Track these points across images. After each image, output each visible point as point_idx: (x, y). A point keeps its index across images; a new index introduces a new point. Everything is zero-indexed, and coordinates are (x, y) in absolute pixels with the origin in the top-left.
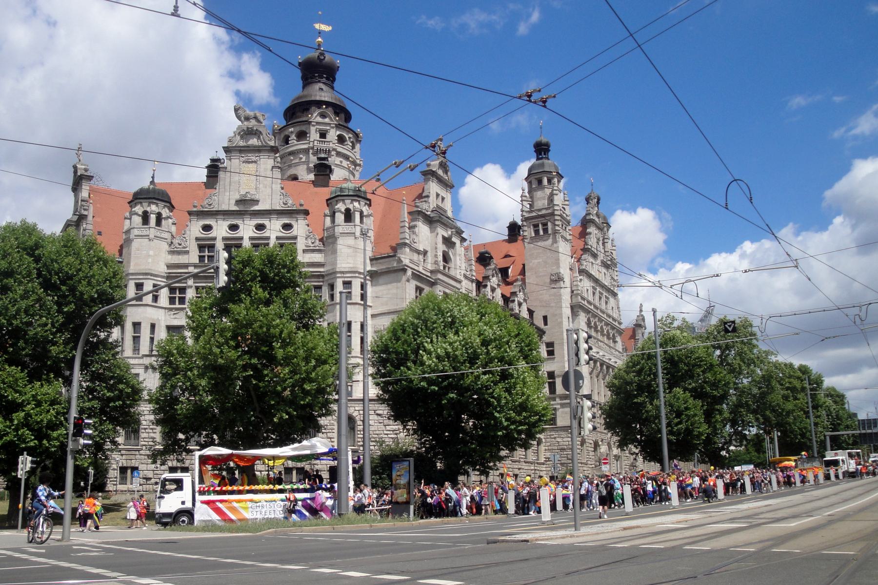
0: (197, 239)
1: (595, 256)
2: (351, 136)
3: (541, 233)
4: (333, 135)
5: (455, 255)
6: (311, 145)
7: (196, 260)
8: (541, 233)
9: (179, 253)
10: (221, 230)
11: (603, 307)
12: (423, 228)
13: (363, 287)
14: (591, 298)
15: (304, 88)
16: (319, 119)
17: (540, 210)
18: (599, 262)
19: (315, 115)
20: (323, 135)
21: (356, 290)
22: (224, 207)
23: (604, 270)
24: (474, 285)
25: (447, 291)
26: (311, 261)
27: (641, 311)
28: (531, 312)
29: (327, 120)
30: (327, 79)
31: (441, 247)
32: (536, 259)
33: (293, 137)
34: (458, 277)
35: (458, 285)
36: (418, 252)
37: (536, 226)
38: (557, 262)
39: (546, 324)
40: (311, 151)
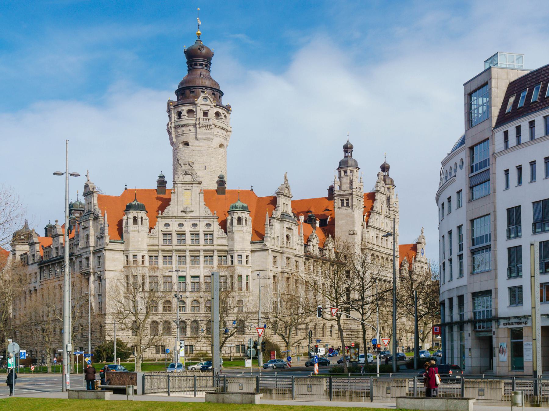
1: (379, 214)
2: (224, 112)
3: (345, 204)
5: (293, 235)
7: (161, 242)
8: (345, 204)
9: (153, 238)
10: (174, 227)
11: (384, 245)
12: (277, 225)
13: (247, 256)
14: (375, 242)
15: (189, 71)
17: (344, 191)
18: (382, 216)
19: (199, 98)
20: (205, 114)
21: (244, 259)
22: (175, 215)
24: (303, 247)
25: (289, 256)
26: (221, 243)
29: (208, 102)
30: (206, 66)
34: (294, 248)
35: (294, 251)
36: (274, 238)
37: (342, 200)
38: (353, 224)
40: (198, 126)
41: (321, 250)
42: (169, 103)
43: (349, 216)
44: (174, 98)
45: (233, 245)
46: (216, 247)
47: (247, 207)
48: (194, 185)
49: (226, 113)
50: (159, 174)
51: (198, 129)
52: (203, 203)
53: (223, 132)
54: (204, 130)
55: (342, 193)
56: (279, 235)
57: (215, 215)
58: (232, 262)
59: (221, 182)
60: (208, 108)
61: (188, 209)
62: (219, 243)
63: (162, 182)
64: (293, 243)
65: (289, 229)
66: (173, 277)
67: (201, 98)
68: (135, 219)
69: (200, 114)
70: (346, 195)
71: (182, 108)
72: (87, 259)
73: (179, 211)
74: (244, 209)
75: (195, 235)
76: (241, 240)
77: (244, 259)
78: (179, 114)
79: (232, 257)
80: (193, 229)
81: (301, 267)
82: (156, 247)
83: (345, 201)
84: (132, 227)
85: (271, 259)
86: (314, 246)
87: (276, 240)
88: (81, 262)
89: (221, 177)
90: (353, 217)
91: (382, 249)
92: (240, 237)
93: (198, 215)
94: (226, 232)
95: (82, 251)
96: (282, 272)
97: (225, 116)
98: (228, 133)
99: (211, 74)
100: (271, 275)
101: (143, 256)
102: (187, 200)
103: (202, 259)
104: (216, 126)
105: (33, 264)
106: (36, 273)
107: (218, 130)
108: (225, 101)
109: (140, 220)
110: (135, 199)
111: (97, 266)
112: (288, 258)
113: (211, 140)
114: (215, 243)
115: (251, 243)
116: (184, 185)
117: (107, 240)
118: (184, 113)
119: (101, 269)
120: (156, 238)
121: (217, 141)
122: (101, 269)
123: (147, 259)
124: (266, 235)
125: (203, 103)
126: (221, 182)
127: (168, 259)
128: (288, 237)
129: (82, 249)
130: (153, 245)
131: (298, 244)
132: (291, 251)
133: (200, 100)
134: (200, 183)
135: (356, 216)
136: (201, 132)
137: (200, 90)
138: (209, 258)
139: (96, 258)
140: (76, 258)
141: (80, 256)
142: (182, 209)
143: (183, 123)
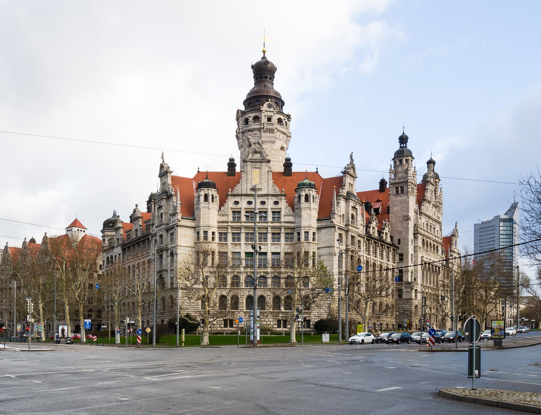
0: (232, 208)
1: (429, 202)
2: (285, 118)
3: (400, 192)
5: (357, 215)
6: (262, 126)
7: (231, 219)
8: (400, 192)
9: (223, 215)
10: (243, 204)
11: (432, 233)
12: (342, 202)
13: (314, 233)
14: (425, 228)
16: (268, 109)
17: (400, 179)
18: (431, 205)
20: (269, 119)
21: (311, 236)
23: (434, 209)
25: (353, 234)
27: (456, 226)
28: (392, 237)
29: (272, 109)
31: (351, 212)
32: (396, 207)
33: (251, 119)
34: (358, 227)
37: (397, 188)
39: (399, 243)
40: (262, 130)
41: (380, 233)
42: (238, 111)
43: (404, 202)
44: (243, 108)
45: (300, 222)
46: (283, 224)
47: (315, 185)
48: (263, 164)
49: (286, 120)
50: (230, 157)
51: (262, 133)
52: (271, 182)
53: (285, 136)
54: (268, 134)
55: (397, 181)
56: (344, 214)
57: (283, 193)
58: (299, 239)
59: (288, 164)
60: (272, 114)
61: (257, 187)
62: (286, 220)
64: (357, 222)
65: (354, 208)
66: (242, 253)
67: (265, 105)
68: (206, 197)
70: (401, 183)
71: (250, 115)
72: (161, 236)
73: (248, 189)
74: (310, 186)
76: (308, 216)
77: (311, 236)
78: (246, 121)
79: (299, 234)
80: (262, 206)
81: (363, 247)
82: (226, 224)
83: (400, 188)
84: (203, 204)
85: (337, 237)
86: (373, 228)
87: (342, 218)
88: (156, 240)
89: (288, 160)
90: (407, 203)
91: (430, 236)
92: (307, 214)
93: (266, 193)
94: (293, 210)
95: (157, 230)
96: (347, 250)
97: (286, 122)
98: (289, 138)
99: (274, 86)
100: (337, 251)
101: (213, 233)
102: (258, 179)
103: (269, 236)
104: (278, 131)
105: (118, 246)
106: (120, 254)
107: (280, 134)
108: (285, 110)
109: (210, 197)
110: (207, 178)
111: (170, 243)
112: (353, 237)
114: (283, 219)
115: (318, 220)
116: (253, 164)
117: (179, 216)
118: (251, 119)
119: (173, 245)
120: (226, 215)
121: (279, 144)
122: (173, 245)
123: (217, 235)
124: (333, 212)
125: (268, 109)
127: (236, 237)
128: (352, 215)
129: (157, 227)
130: (223, 222)
131: (361, 225)
132: (355, 229)
133: (265, 107)
134: (269, 161)
135: (410, 202)
136: (265, 136)
137: (265, 99)
139: (169, 235)
140: (152, 237)
141: (155, 235)
142: (250, 187)
143: (250, 128)
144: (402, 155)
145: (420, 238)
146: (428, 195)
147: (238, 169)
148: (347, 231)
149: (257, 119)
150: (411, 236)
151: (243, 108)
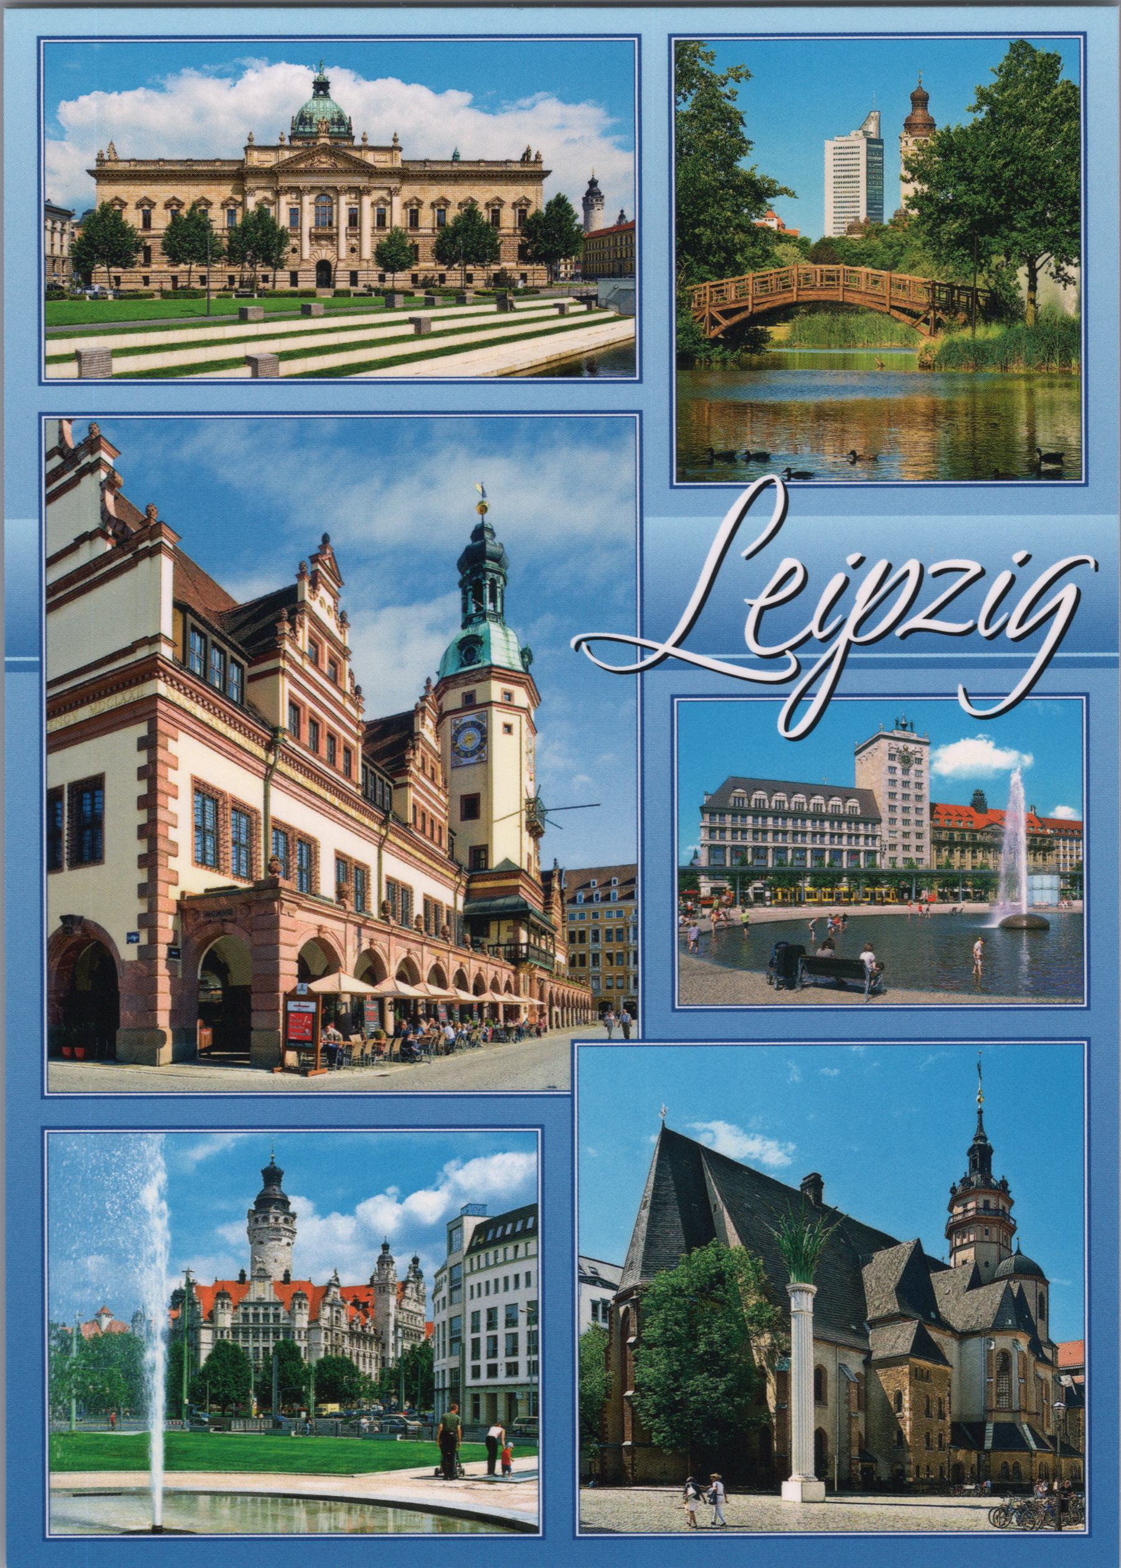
4: (281, 1219)
10: (251, 1310)
12: (328, 1309)
20: (277, 1219)
31: (335, 1314)
44: (253, 1208)
59: (287, 1275)
63: (242, 1275)
69: (272, 1220)
75: (266, 1316)
78: (257, 1220)
85: (323, 1335)
96: (331, 1345)
100: (323, 1347)
108: (292, 1209)
113: (280, 1240)
126: (287, 1275)
133: (273, 1210)
138: (276, 1334)
144: (384, 1261)
145: (400, 1330)
146: (408, 1292)
147: (248, 1278)
148: (331, 1330)
149: (266, 1219)
150: (392, 1328)
151: (253, 1208)
